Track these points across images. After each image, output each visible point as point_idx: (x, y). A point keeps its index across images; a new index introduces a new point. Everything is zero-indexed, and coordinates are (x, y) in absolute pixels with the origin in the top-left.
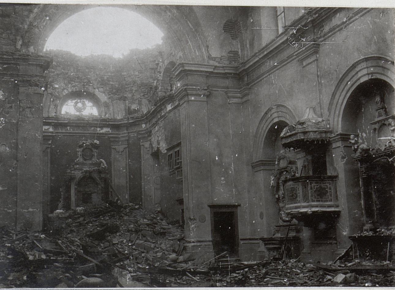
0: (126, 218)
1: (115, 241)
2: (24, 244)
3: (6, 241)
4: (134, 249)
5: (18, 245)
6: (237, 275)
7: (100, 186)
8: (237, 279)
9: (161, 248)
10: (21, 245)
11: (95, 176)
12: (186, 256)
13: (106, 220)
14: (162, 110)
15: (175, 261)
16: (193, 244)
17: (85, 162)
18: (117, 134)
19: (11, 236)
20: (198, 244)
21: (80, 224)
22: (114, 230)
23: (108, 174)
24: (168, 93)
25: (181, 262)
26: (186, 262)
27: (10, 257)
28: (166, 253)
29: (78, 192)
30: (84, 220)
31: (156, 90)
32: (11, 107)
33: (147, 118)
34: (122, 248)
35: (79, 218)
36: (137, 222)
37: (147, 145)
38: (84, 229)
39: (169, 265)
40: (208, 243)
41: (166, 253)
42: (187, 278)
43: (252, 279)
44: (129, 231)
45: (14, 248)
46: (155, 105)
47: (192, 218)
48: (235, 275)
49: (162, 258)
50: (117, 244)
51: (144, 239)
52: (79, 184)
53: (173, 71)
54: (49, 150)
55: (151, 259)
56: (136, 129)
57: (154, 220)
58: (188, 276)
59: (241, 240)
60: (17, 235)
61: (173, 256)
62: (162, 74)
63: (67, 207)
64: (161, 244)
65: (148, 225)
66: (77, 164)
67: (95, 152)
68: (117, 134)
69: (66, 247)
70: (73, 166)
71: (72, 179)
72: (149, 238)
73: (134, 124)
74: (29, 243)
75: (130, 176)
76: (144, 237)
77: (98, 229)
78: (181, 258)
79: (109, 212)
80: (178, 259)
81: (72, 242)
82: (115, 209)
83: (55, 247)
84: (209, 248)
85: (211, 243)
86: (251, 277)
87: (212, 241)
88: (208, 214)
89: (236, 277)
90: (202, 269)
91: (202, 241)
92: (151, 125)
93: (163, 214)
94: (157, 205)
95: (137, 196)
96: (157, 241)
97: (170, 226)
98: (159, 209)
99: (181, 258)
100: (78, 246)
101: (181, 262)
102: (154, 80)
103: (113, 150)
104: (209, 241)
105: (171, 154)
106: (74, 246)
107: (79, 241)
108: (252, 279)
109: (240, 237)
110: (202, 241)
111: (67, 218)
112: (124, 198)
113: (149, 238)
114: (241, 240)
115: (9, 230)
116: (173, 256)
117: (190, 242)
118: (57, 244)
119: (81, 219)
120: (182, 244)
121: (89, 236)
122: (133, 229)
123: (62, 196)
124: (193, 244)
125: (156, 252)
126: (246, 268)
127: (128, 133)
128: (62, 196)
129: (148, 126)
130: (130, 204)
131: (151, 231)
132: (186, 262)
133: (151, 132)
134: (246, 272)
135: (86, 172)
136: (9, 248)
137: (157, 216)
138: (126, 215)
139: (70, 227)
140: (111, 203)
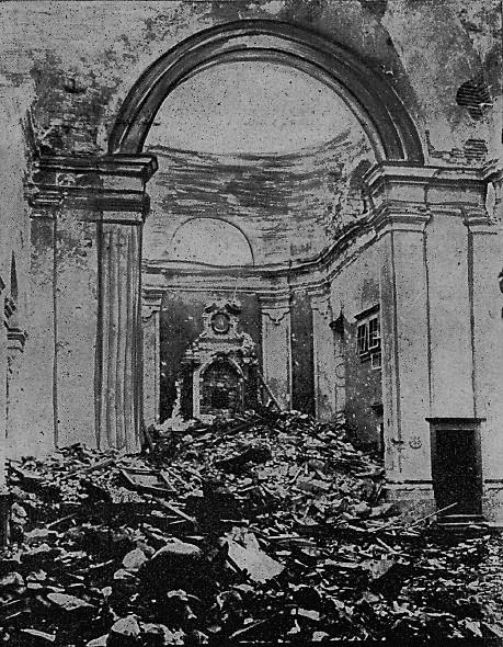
0: (282, 435)
1: (262, 475)
2: (107, 476)
3: (79, 469)
4: (294, 491)
5: (97, 479)
6: (468, 547)
7: (241, 380)
8: (465, 553)
9: (340, 490)
10: (102, 477)
11: (234, 361)
12: (387, 506)
13: (250, 440)
14: (347, 246)
15: (364, 515)
16: (398, 487)
17: (216, 337)
18: (272, 289)
19: (87, 462)
20: (409, 486)
21: (206, 445)
22: (261, 456)
23: (255, 358)
24: (359, 218)
25: (376, 518)
26: (384, 517)
27: (83, 496)
28: (350, 500)
29: (205, 388)
30: (213, 438)
31: (338, 211)
32: (90, 245)
33: (322, 261)
34: (274, 489)
35: (203, 433)
36: (300, 443)
37: (324, 307)
38: (210, 454)
39: (351, 522)
40: (424, 486)
41: (350, 500)
42: (377, 547)
43: (493, 554)
44: (287, 459)
45: (91, 481)
46: (336, 238)
47: (397, 440)
48: (463, 545)
49: (341, 510)
50: (266, 481)
51: (312, 474)
52: (205, 376)
53: (365, 178)
54: (157, 316)
55: (323, 511)
56: (307, 279)
57: (333, 441)
58: (380, 545)
59: (486, 482)
60: (97, 460)
61: (362, 506)
62: (348, 183)
63: (187, 412)
64: (340, 484)
65: (319, 449)
66: (202, 340)
67: (234, 320)
68: (272, 289)
69: (176, 485)
70: (197, 343)
71: (195, 365)
72: (320, 473)
73: (301, 271)
74: (114, 475)
75: (294, 364)
76: (313, 470)
77: (236, 453)
78: (376, 511)
79: (257, 424)
80: (370, 511)
81: (187, 476)
82: (269, 420)
83: (157, 483)
84: (427, 494)
85: (431, 486)
86: (491, 551)
87: (502, 482)
88: (425, 434)
89: (466, 549)
90: (410, 532)
91: (416, 482)
92: (330, 272)
93: (349, 432)
94: (339, 415)
95: (305, 393)
96: (335, 478)
97: (360, 453)
98: (343, 422)
99: (376, 511)
100: (197, 482)
101: (376, 518)
102: (336, 194)
103: (264, 316)
104: (428, 482)
105: (364, 326)
106: (189, 482)
107: (198, 474)
108: (493, 554)
109: (484, 478)
110: (416, 482)
111: (185, 433)
112: (282, 402)
113: (320, 473)
114: (486, 482)
115: (84, 451)
116: (362, 506)
117: (392, 483)
118: (160, 478)
119: (208, 436)
120: (378, 486)
121: (217, 466)
122: (294, 457)
123: (179, 395)
124: (398, 487)
125: (333, 498)
126: (486, 534)
127: (291, 287)
128: (179, 395)
129: (325, 274)
130: (293, 412)
131: (324, 460)
132: (384, 517)
133: (329, 285)
134: (485, 542)
135: (219, 354)
136: (83, 483)
137: (339, 435)
138: (284, 431)
139: (189, 449)
140: (258, 408)
